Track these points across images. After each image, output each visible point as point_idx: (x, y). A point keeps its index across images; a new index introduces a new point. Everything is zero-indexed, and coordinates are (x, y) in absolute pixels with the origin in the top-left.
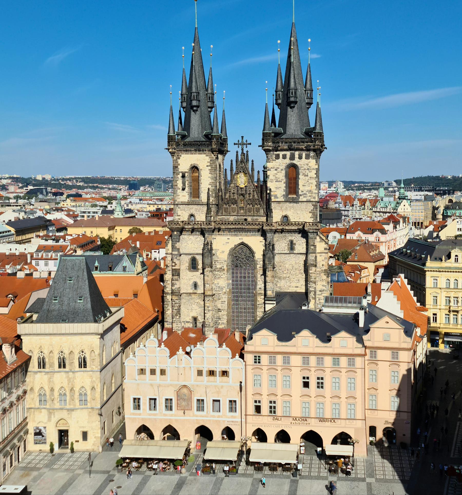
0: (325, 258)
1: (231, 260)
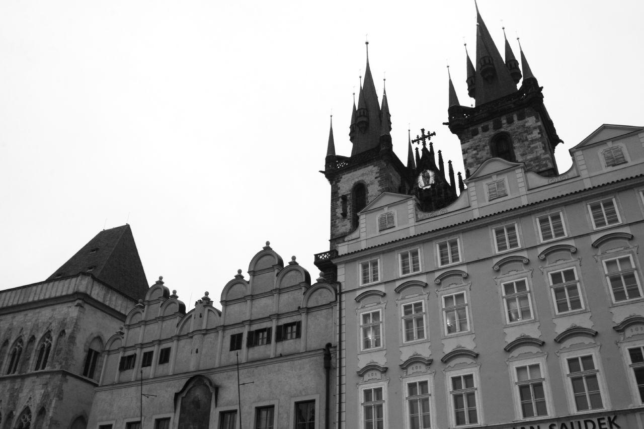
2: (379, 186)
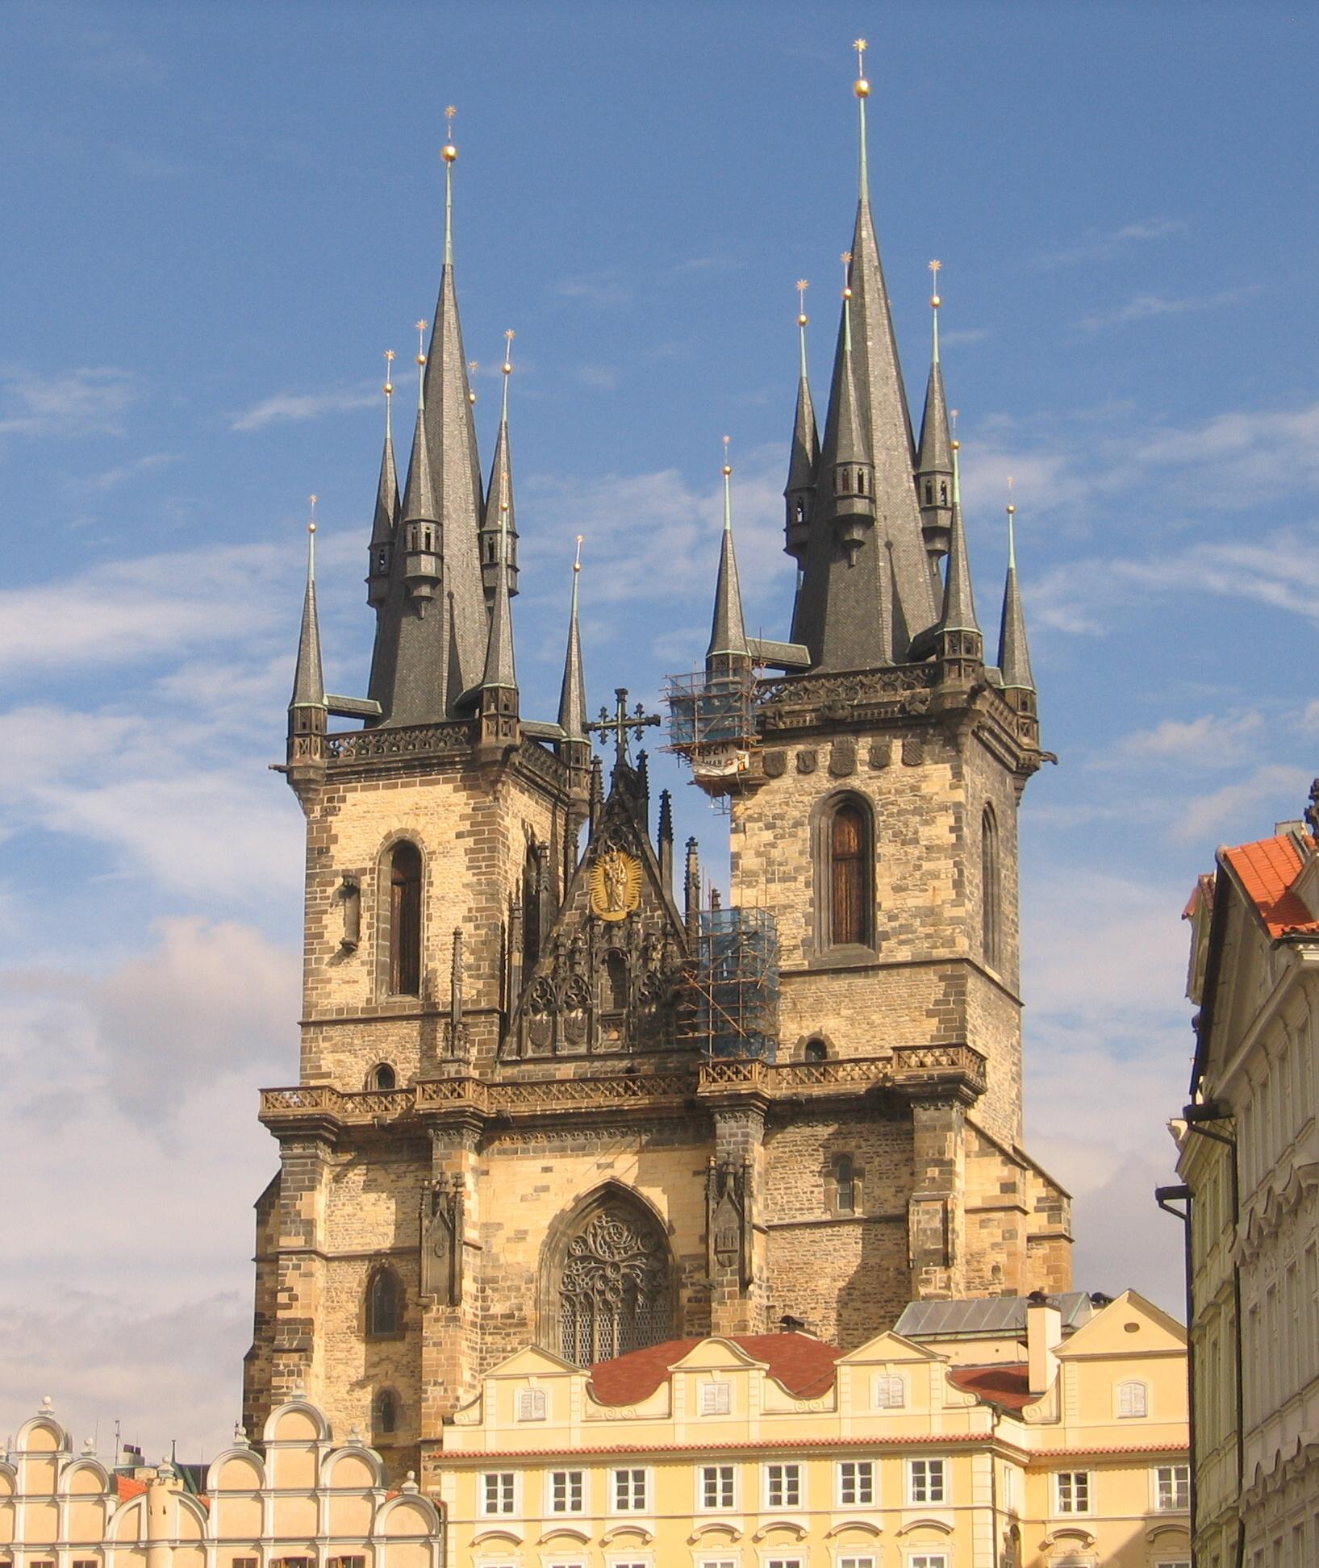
0: (1009, 1235)
1: (557, 1274)
2: (469, 868)
